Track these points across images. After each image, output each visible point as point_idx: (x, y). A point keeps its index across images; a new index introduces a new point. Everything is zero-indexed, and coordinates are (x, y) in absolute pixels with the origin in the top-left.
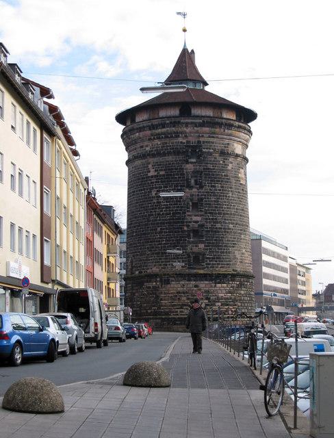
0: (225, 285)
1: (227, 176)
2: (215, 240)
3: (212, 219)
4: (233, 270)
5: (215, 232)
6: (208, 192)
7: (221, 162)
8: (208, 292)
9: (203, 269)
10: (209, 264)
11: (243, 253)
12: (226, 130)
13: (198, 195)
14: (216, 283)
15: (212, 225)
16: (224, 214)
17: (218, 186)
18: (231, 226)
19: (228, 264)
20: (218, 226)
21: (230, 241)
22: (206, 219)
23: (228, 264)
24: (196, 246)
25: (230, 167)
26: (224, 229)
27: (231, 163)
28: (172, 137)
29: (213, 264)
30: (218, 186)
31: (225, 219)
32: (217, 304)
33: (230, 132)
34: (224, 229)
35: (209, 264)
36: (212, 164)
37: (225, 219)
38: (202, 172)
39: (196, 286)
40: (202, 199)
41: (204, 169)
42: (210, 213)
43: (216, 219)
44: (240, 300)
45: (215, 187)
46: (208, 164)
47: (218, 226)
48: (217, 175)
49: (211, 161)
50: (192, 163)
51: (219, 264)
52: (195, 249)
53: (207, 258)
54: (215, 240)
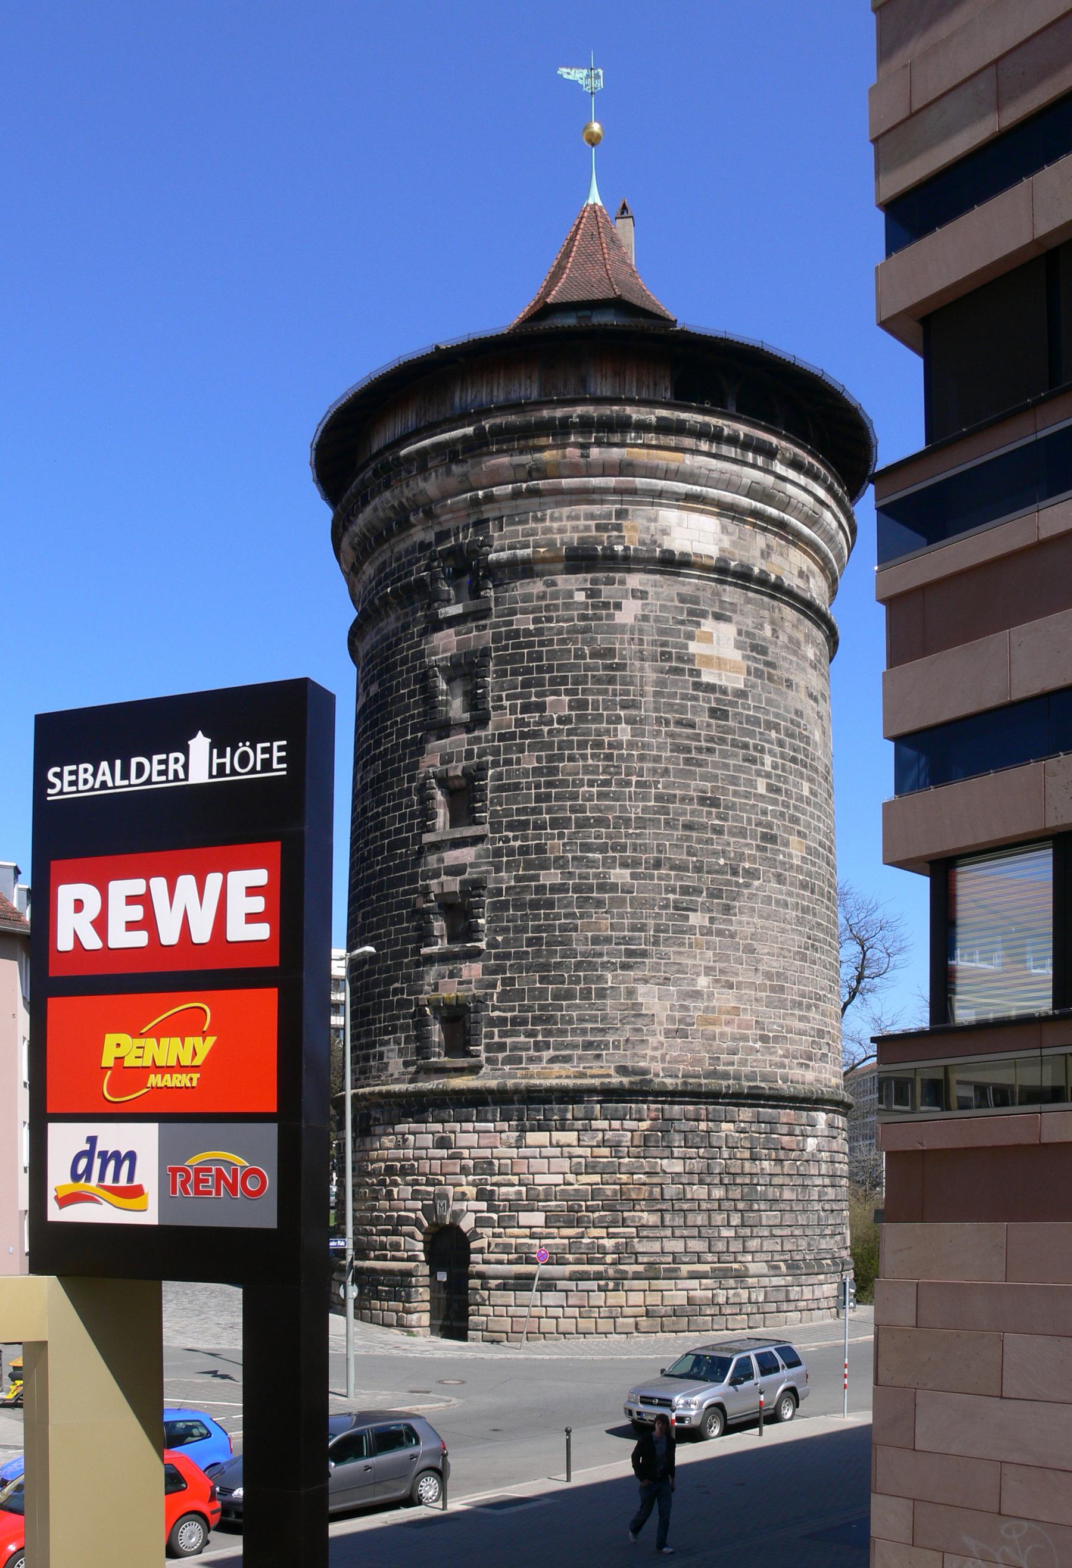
0: (571, 1137)
1: (610, 653)
2: (530, 942)
3: (524, 851)
4: (622, 1070)
5: (535, 905)
6: (512, 736)
7: (580, 597)
8: (485, 1166)
9: (474, 1070)
10: (502, 1047)
11: (696, 995)
12: (595, 452)
13: (469, 754)
14: (523, 1130)
15: (518, 879)
16: (582, 824)
17: (558, 704)
18: (620, 875)
19: (588, 1046)
20: (551, 877)
21: (608, 940)
22: (498, 853)
23: (588, 1046)
24: (452, 975)
25: (629, 613)
26: (577, 889)
27: (640, 594)
28: (391, 533)
29: (515, 1047)
30: (558, 704)
31: (586, 847)
32: (525, 1218)
33: (616, 453)
34: (577, 889)
35: (502, 1047)
36: (538, 609)
37: (586, 847)
38: (485, 653)
39: (442, 1143)
40: (482, 768)
41: (496, 638)
42: (511, 827)
43: (540, 849)
44: (651, 1199)
45: (541, 707)
46: (513, 612)
47: (551, 877)
48: (552, 655)
49: (527, 598)
50: (452, 622)
51: (547, 1046)
52: (450, 991)
53: (492, 1022)
54: (530, 942)
